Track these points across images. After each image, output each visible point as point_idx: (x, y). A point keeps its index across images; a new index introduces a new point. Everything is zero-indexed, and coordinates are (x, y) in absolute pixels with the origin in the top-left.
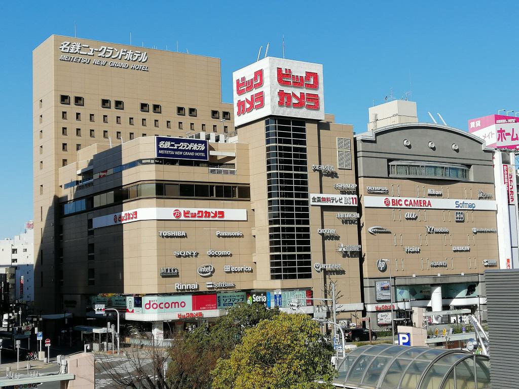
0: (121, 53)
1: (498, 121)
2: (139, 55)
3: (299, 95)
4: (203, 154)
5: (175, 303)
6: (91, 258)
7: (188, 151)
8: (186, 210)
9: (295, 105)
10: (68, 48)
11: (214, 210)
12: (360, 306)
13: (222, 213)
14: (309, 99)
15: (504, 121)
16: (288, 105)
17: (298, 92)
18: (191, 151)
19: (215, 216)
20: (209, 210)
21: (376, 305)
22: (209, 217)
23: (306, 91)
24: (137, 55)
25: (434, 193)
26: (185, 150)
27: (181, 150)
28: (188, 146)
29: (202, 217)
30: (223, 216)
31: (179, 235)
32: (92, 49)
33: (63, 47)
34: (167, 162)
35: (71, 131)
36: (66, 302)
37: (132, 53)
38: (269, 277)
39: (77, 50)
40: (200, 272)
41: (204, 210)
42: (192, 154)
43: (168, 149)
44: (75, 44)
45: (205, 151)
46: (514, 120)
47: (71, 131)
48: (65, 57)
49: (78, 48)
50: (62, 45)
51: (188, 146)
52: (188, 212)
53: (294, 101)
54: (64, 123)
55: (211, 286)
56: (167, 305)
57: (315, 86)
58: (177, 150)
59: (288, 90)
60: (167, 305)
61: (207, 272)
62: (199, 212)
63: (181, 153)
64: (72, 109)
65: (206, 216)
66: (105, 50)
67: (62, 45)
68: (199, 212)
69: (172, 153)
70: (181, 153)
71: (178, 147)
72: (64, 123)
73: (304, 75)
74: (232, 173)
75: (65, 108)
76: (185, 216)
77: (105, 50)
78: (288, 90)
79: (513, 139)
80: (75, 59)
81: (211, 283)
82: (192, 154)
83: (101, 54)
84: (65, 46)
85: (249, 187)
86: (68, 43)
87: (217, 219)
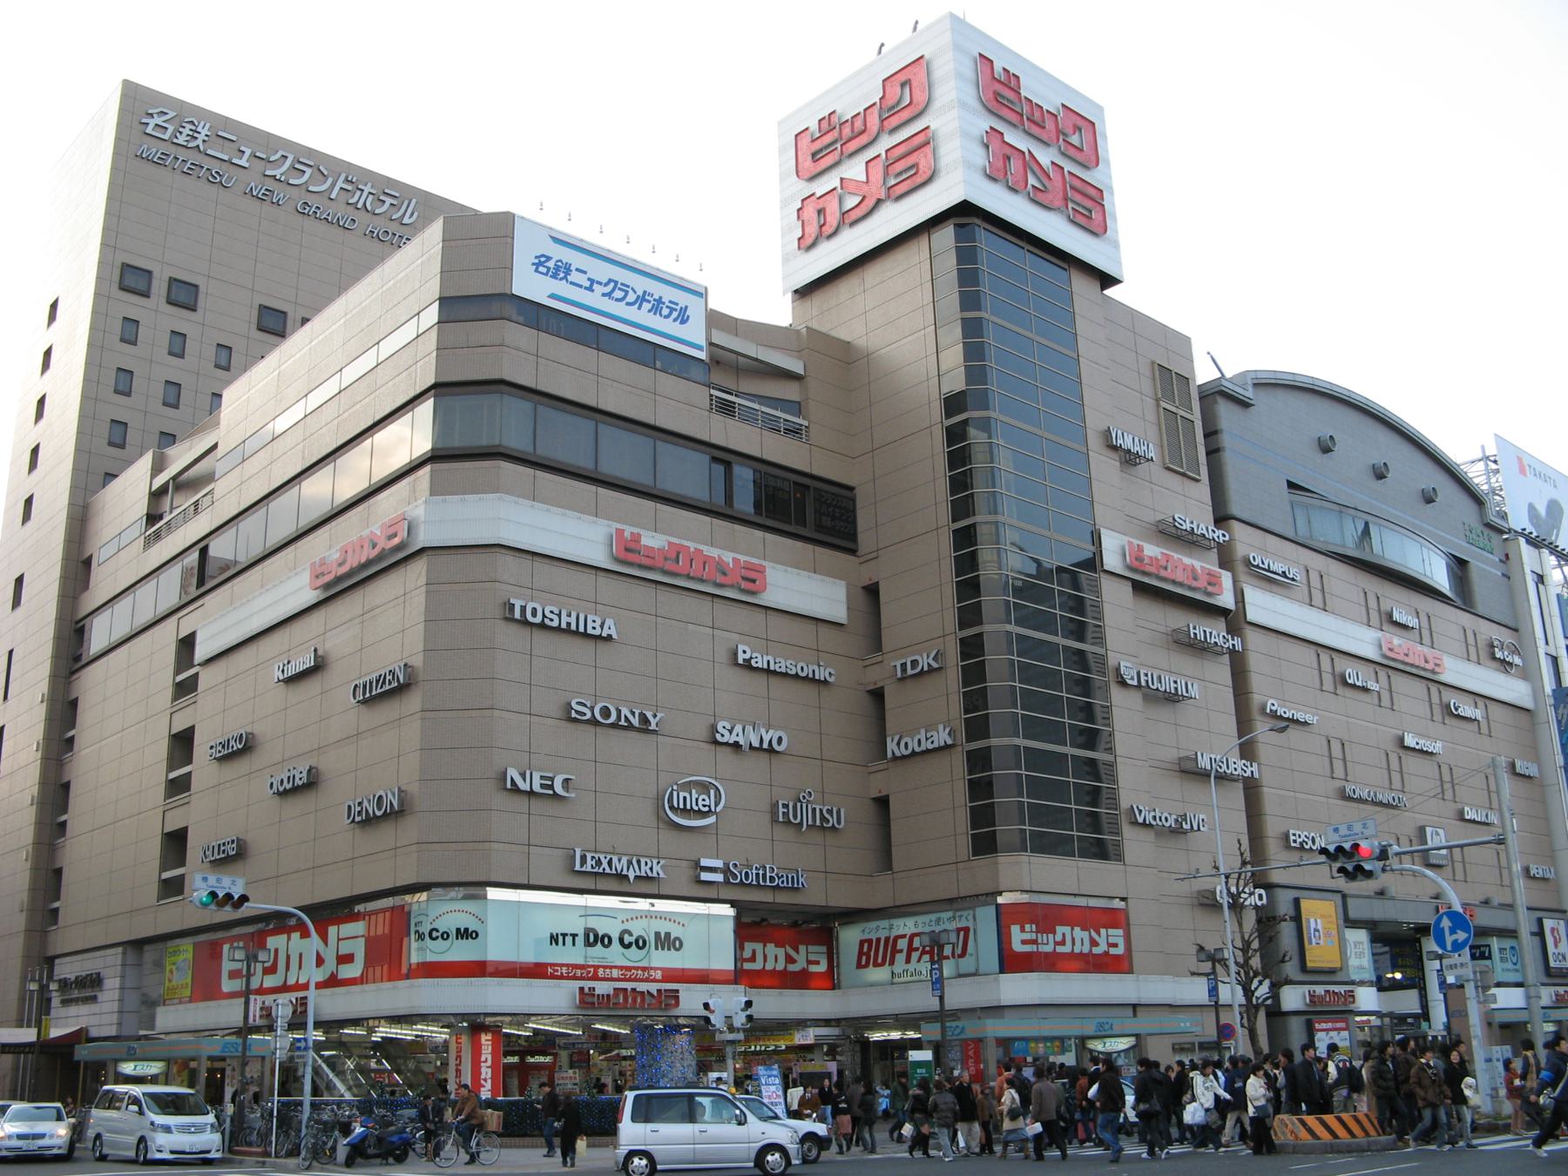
0: (340, 184)
2: (395, 202)
6: (178, 787)
10: (171, 128)
13: (752, 580)
17: (1045, 157)
24: (389, 201)
31: (590, 631)
32: (248, 152)
33: (152, 122)
35: (149, 388)
36: (64, 985)
37: (374, 192)
38: (964, 844)
39: (199, 142)
40: (672, 807)
44: (192, 122)
47: (149, 388)
48: (155, 149)
49: (201, 137)
50: (151, 115)
54: (126, 356)
55: (719, 877)
59: (1014, 138)
61: (701, 814)
64: (157, 316)
66: (288, 163)
67: (151, 115)
72: (126, 356)
74: (794, 431)
75: (132, 306)
77: (288, 163)
78: (1014, 138)
80: (188, 165)
81: (719, 863)
83: (277, 173)
84: (159, 120)
85: (853, 500)
86: (172, 114)
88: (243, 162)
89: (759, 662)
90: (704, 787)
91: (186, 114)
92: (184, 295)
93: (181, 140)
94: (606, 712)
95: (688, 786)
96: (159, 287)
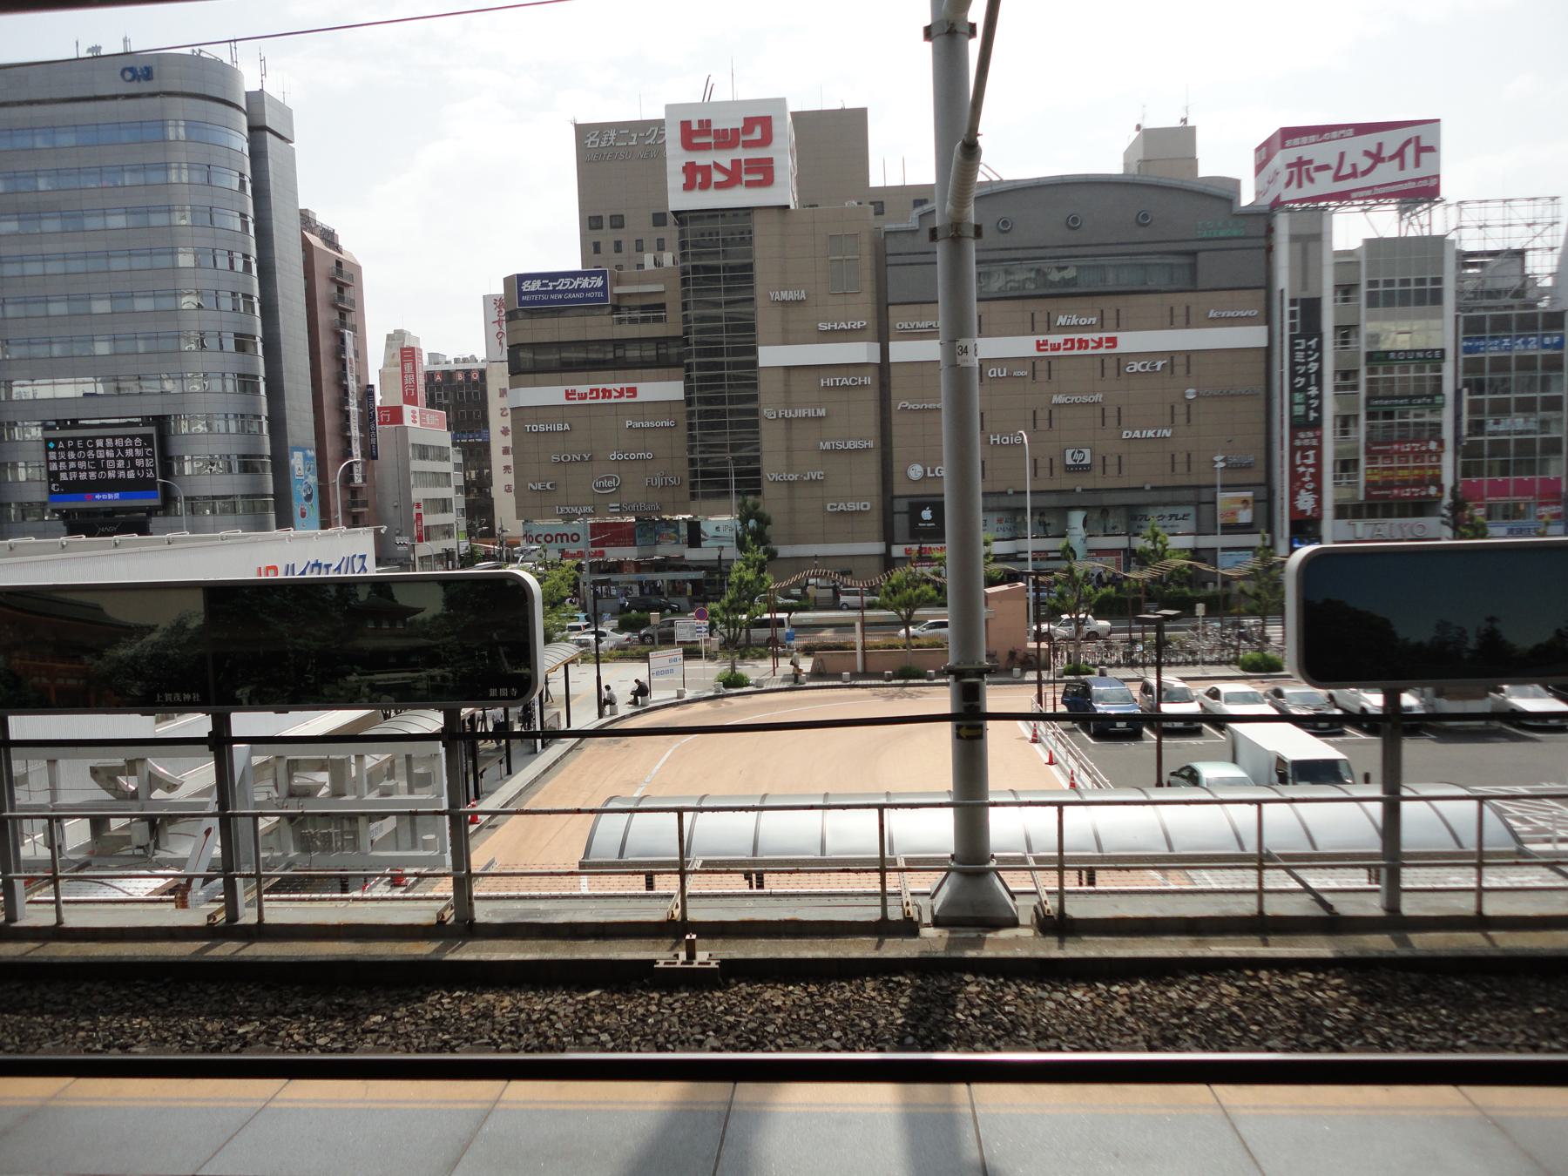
1: (1288, 142)
3: (728, 166)
4: (600, 294)
5: (562, 536)
7: (573, 291)
8: (570, 388)
9: (719, 186)
11: (618, 386)
12: (877, 548)
13: (633, 391)
14: (748, 171)
15: (1313, 138)
16: (705, 185)
17: (725, 158)
18: (579, 290)
19: (621, 394)
20: (609, 387)
21: (908, 546)
22: (610, 397)
23: (741, 154)
25: (1074, 321)
26: (567, 291)
27: (560, 292)
28: (571, 283)
29: (597, 397)
30: (635, 395)
32: (635, 136)
34: (532, 314)
41: (600, 387)
42: (579, 296)
43: (537, 292)
45: (604, 288)
46: (1351, 131)
51: (571, 283)
52: (573, 392)
53: (717, 177)
56: (549, 539)
57: (766, 140)
58: (554, 291)
59: (702, 159)
60: (549, 539)
61: (608, 488)
62: (591, 391)
63: (560, 296)
65: (604, 397)
68: (591, 391)
69: (544, 297)
70: (560, 296)
71: (554, 286)
73: (740, 125)
74: (658, 319)
76: (567, 398)
78: (702, 159)
79: (1337, 178)
82: (579, 296)
84: (592, 139)
87: (624, 400)
88: (634, 143)
89: (637, 425)
90: (609, 478)
91: (602, 128)
92: (618, 222)
93: (603, 144)
94: (566, 458)
95: (602, 479)
96: (606, 223)
